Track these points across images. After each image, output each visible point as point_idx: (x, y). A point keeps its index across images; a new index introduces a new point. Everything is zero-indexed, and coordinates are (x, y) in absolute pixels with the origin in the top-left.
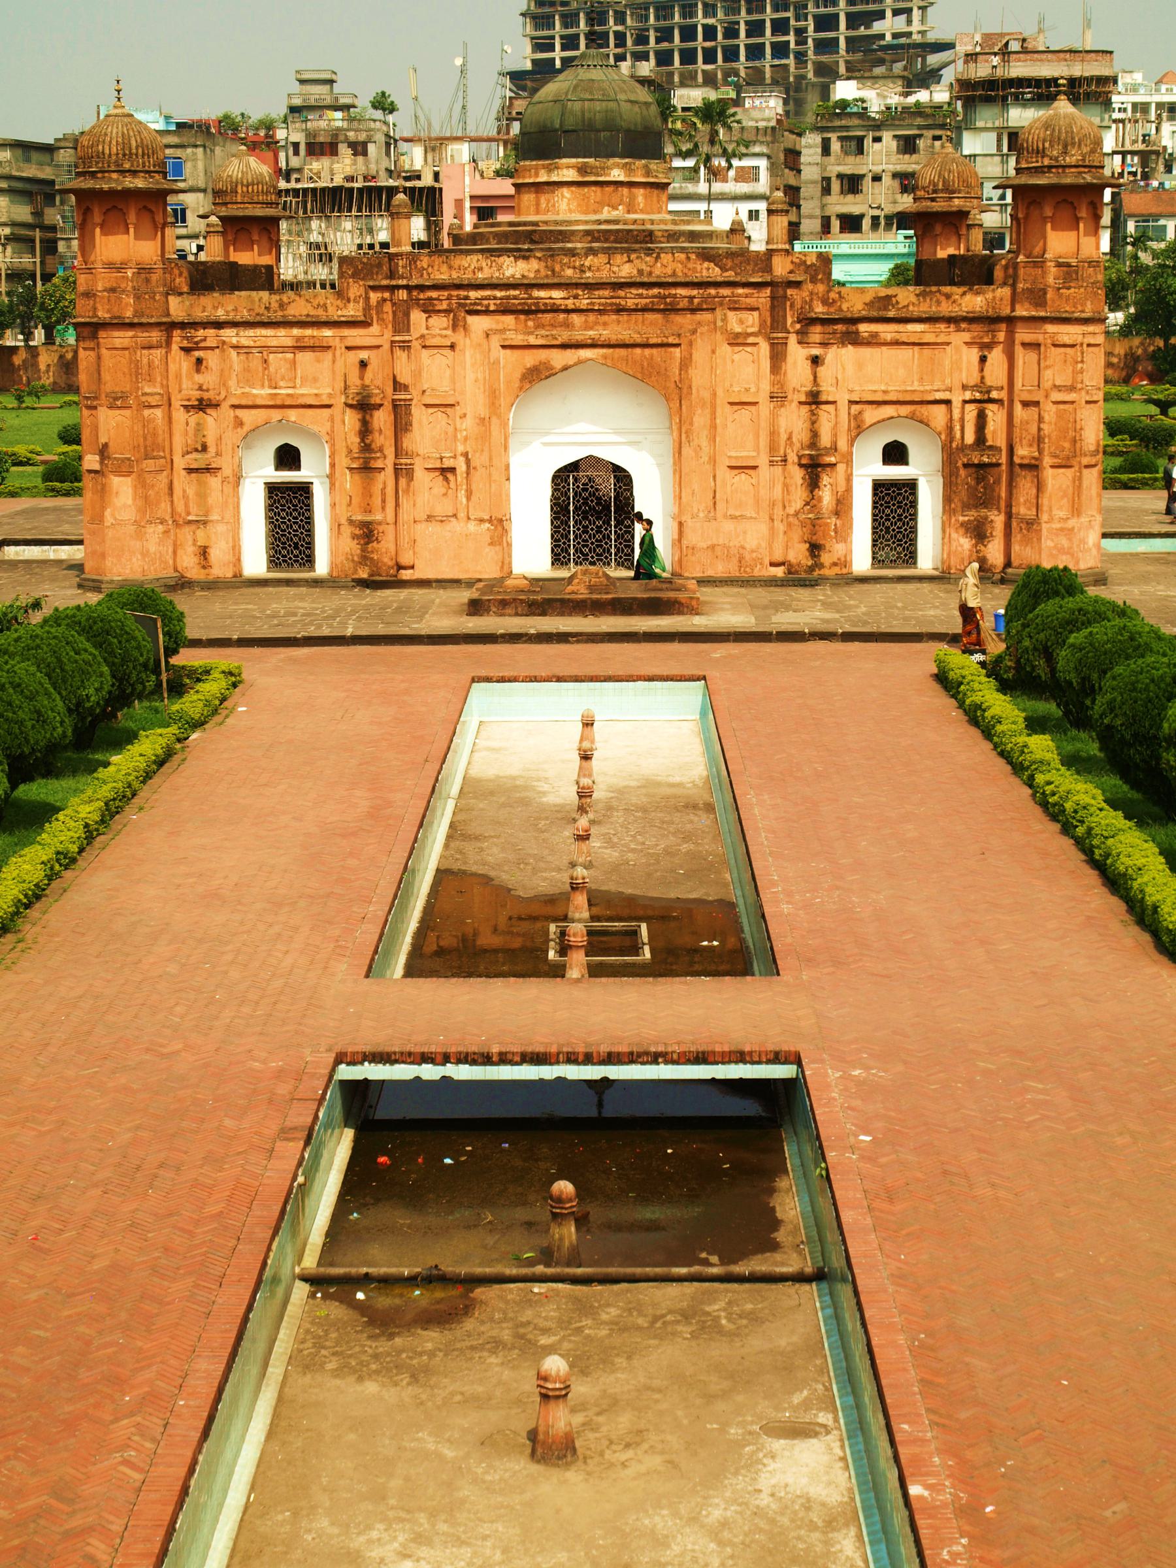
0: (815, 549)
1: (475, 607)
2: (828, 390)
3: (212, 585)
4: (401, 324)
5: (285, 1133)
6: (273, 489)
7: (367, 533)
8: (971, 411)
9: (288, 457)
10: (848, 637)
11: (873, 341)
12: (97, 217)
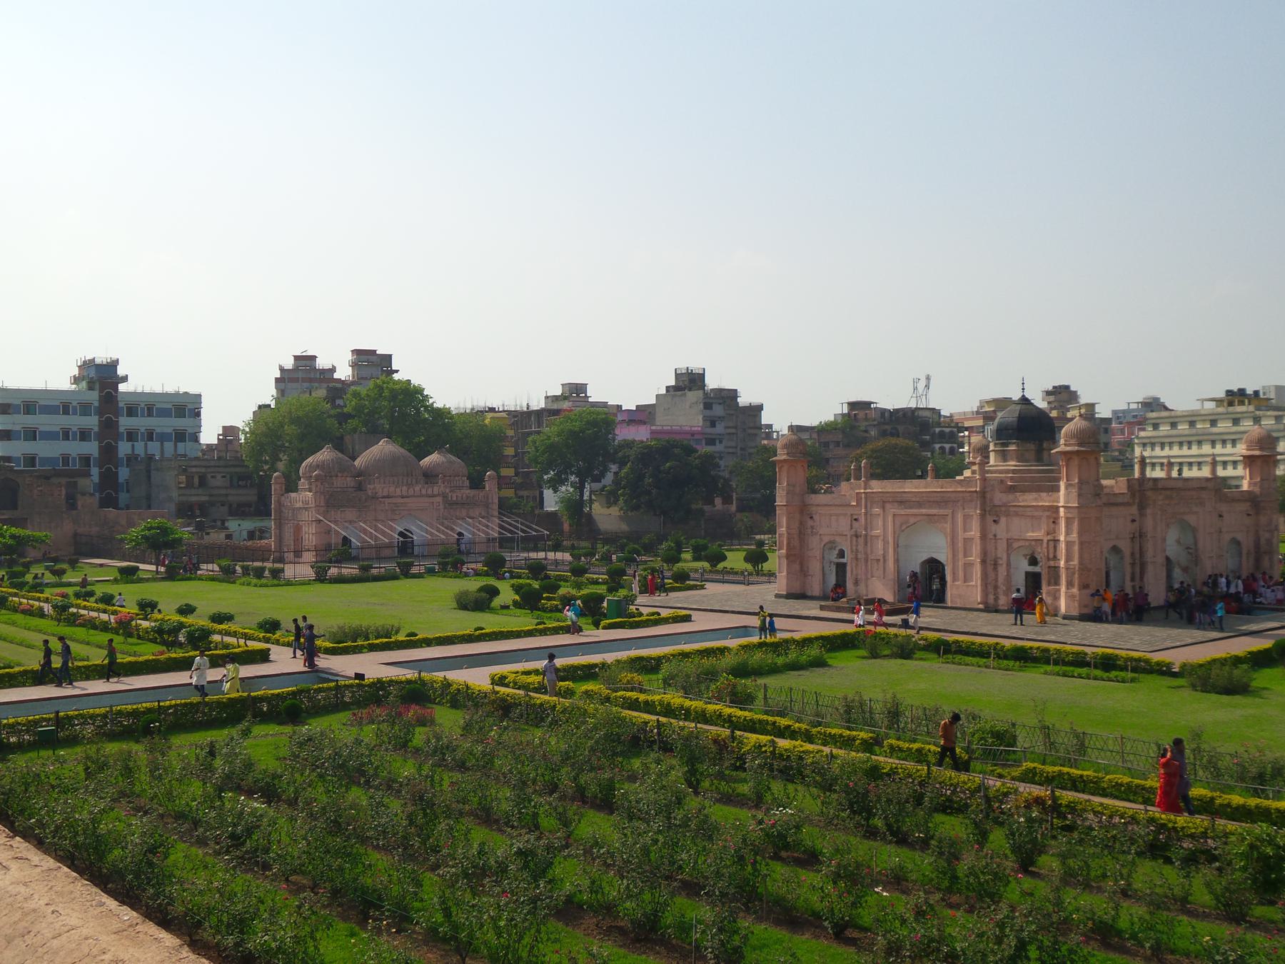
0: (996, 599)
1: (822, 608)
8: (1051, 544)
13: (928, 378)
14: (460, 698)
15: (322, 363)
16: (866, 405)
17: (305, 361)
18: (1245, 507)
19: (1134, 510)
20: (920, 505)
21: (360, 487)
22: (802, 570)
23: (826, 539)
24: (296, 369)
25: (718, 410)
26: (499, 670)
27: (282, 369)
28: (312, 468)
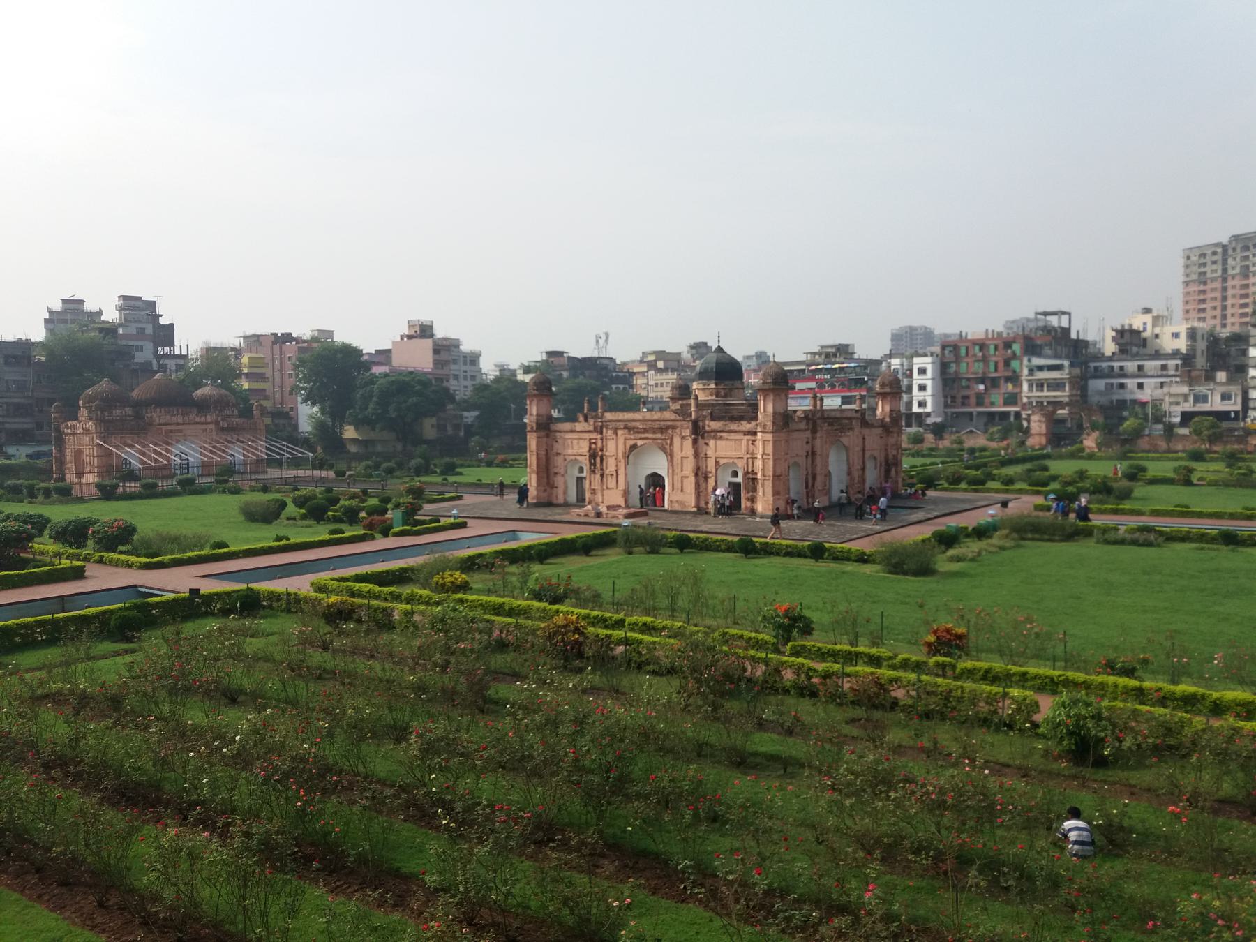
2: (710, 453)
4: (601, 433)
11: (721, 438)
13: (607, 335)
14: (292, 604)
15: (90, 306)
16: (560, 354)
17: (73, 305)
18: (879, 431)
19: (808, 434)
20: (645, 431)
21: (138, 417)
22: (548, 483)
24: (63, 312)
25: (444, 356)
26: (324, 576)
27: (51, 312)
28: (91, 399)
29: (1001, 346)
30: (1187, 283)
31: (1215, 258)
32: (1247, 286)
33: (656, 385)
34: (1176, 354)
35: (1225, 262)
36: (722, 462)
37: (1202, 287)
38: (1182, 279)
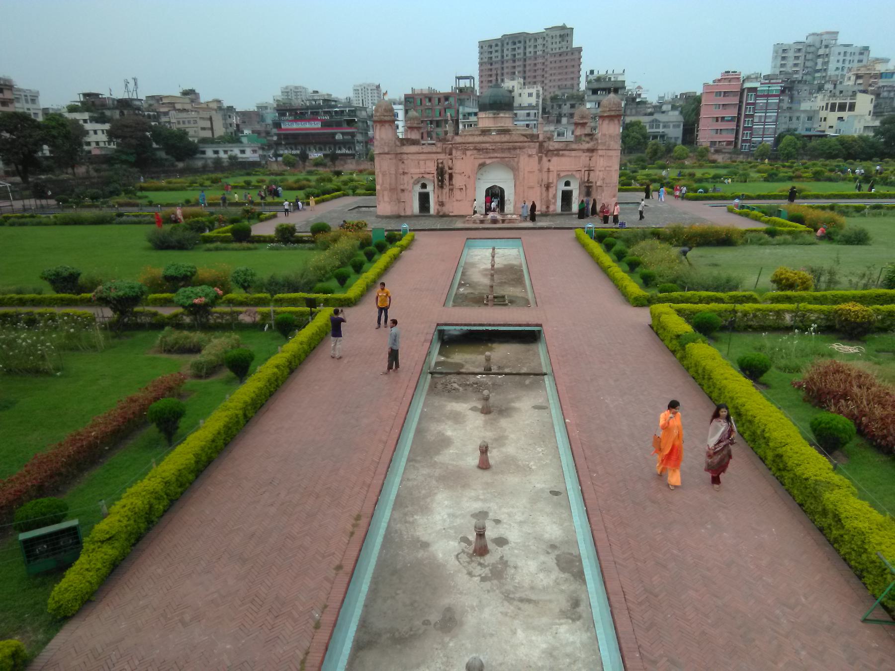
0: (548, 207)
2: (552, 168)
3: (406, 217)
4: (451, 154)
5: (425, 341)
6: (421, 194)
7: (442, 204)
9: (424, 186)
10: (555, 228)
11: (563, 155)
12: (378, 127)
23: (416, 177)
29: (443, 100)
30: (481, 64)
31: (497, 48)
32: (514, 67)
33: (179, 123)
34: (530, 107)
35: (503, 51)
36: (562, 174)
37: (489, 67)
38: (478, 61)
